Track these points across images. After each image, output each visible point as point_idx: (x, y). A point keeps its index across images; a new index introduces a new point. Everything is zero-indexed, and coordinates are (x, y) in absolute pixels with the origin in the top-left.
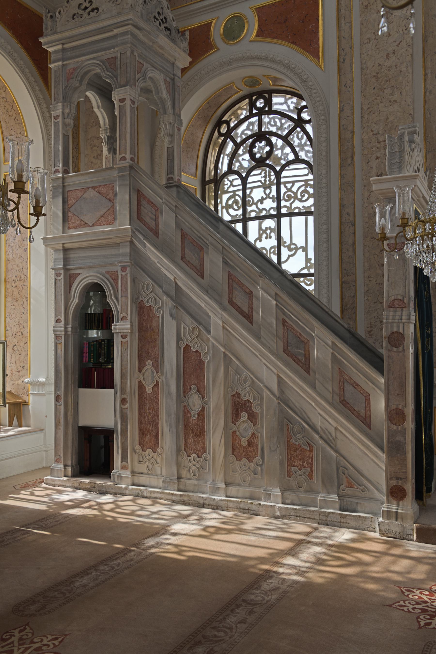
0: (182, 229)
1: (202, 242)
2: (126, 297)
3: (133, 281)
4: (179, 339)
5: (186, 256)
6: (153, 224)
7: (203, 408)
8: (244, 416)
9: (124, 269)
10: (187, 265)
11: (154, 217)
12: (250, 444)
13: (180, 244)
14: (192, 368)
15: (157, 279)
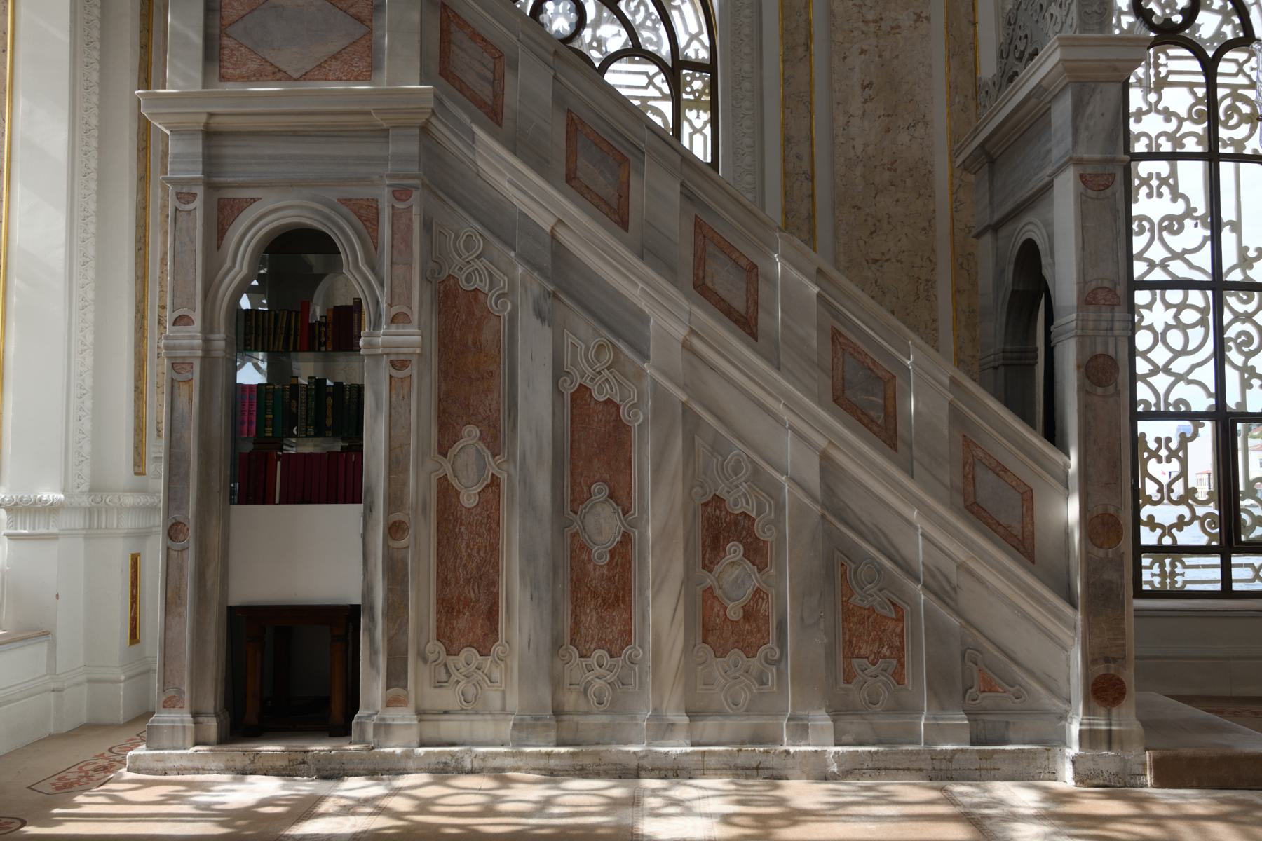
0: (569, 111)
1: (626, 144)
2: (409, 264)
3: (427, 226)
4: (559, 372)
5: (579, 174)
6: (486, 92)
7: (626, 539)
8: (734, 550)
9: (401, 193)
10: (582, 195)
11: (490, 76)
12: (749, 614)
13: (563, 145)
14: (595, 444)
15: (501, 224)
